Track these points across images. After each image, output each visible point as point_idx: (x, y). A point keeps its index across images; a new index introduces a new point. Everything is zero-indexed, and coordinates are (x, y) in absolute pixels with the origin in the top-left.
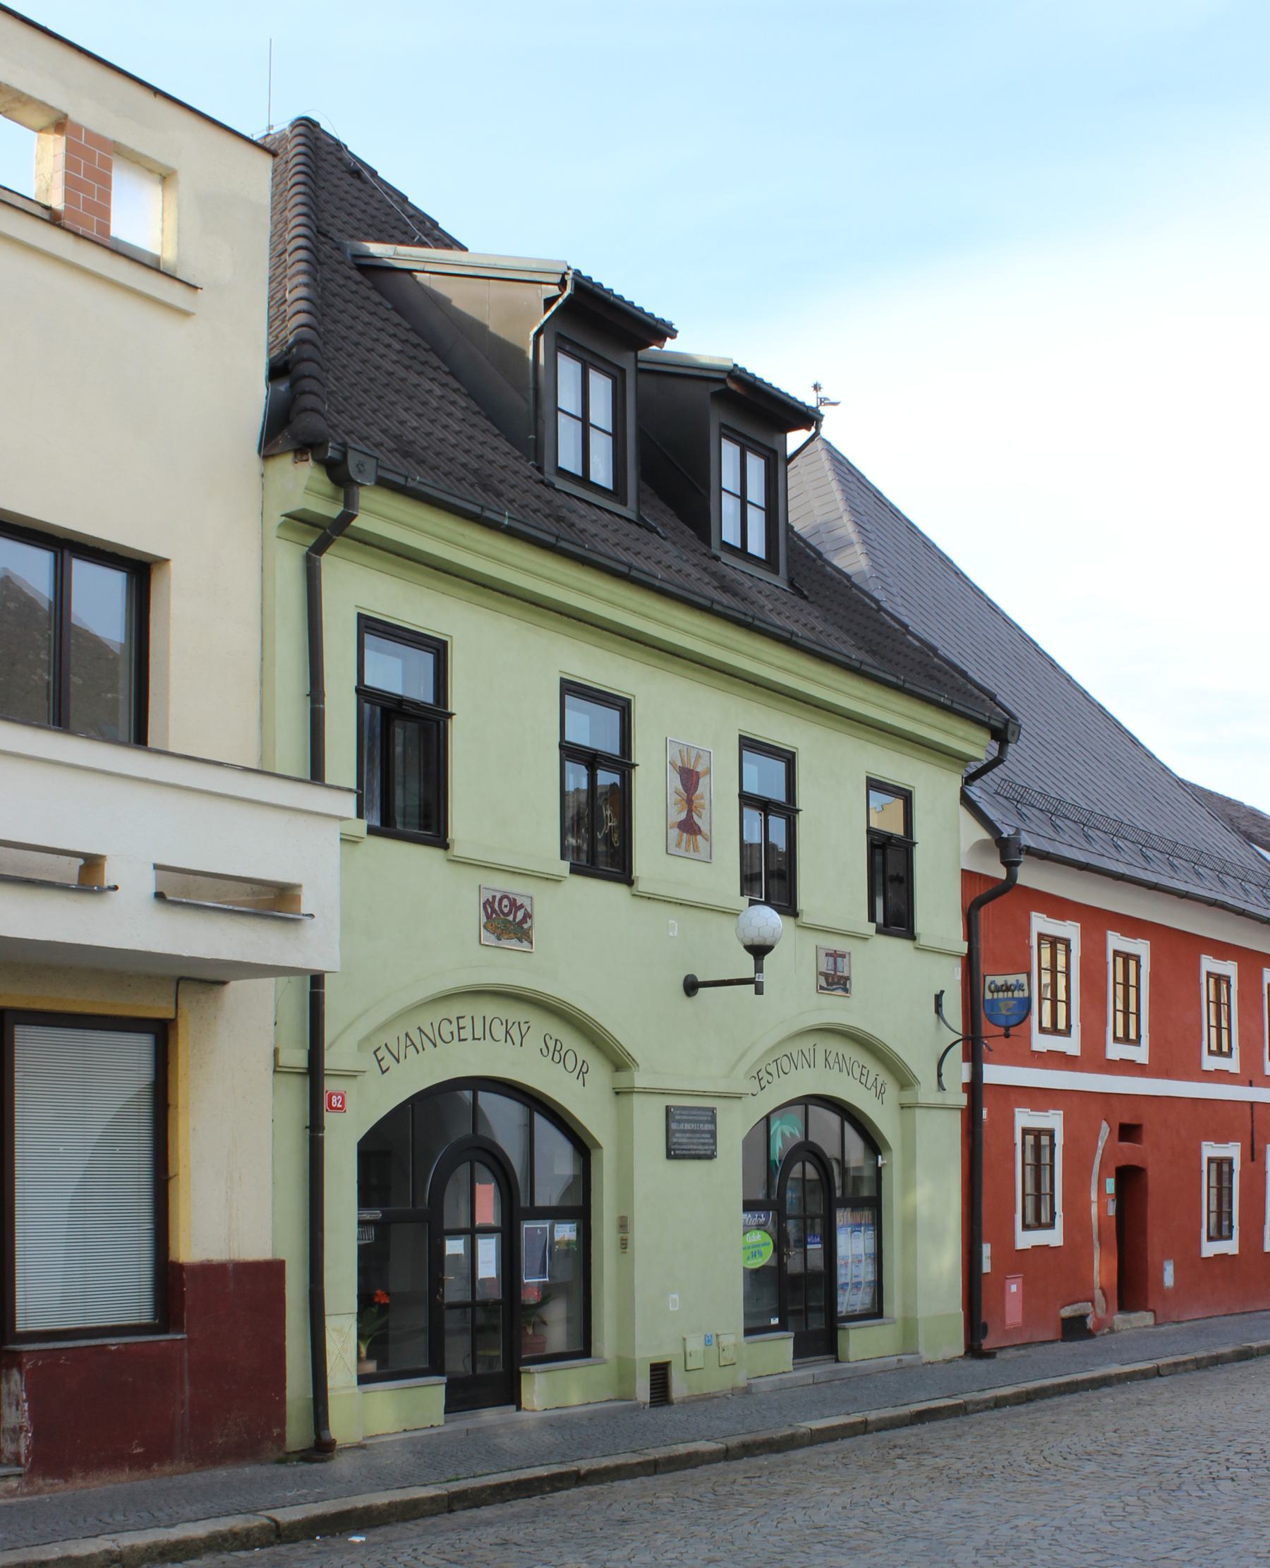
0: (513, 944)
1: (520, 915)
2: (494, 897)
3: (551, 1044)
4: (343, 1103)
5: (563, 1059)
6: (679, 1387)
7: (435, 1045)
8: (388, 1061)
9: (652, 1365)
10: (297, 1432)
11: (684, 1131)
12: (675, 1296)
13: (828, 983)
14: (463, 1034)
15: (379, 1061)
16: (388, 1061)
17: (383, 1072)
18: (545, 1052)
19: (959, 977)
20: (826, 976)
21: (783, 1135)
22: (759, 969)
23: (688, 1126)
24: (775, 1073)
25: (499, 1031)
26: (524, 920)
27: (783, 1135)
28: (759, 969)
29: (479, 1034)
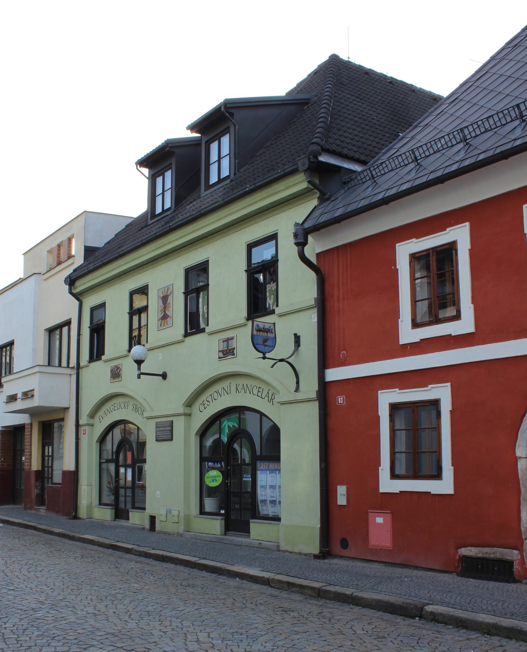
3: (135, 406)
5: (138, 411)
11: (160, 431)
12: (158, 492)
13: (224, 355)
19: (316, 320)
20: (223, 351)
21: (229, 427)
22: (139, 369)
23: (161, 429)
24: (211, 401)
27: (229, 427)
28: (139, 369)
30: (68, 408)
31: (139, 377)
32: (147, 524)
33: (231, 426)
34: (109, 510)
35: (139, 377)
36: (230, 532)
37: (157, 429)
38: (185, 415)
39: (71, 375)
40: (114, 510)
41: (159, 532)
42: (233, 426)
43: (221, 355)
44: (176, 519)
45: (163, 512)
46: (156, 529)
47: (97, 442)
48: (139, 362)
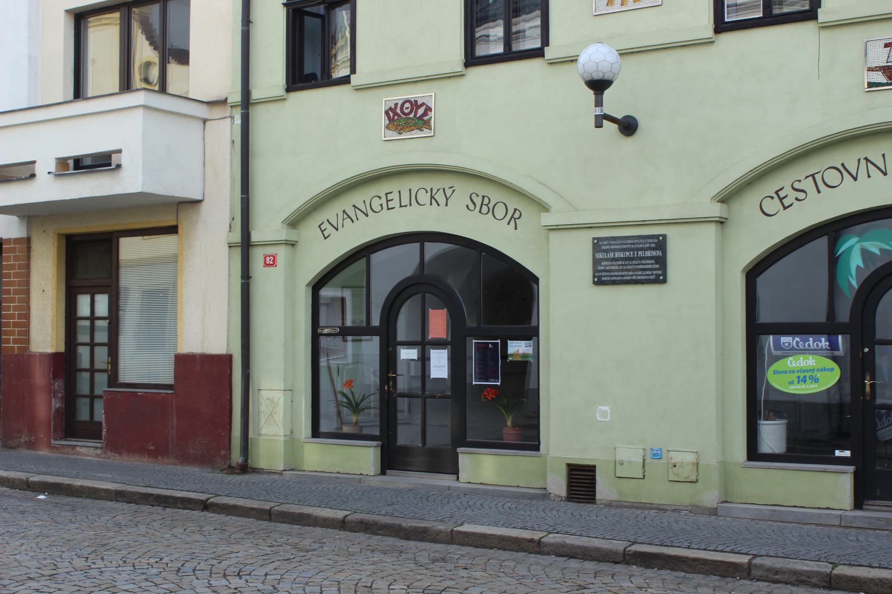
0: (416, 134)
1: (421, 111)
2: (396, 105)
3: (478, 201)
4: (274, 261)
6: (604, 489)
7: (367, 215)
8: (330, 230)
9: (569, 465)
10: (236, 457)
14: (391, 205)
15: (322, 231)
16: (330, 230)
17: (325, 238)
18: (471, 206)
22: (599, 103)
25: (424, 198)
26: (425, 114)
27: (865, 253)
28: (599, 103)
29: (405, 201)
30: (200, 201)
31: (599, 125)
32: (558, 485)
33: (877, 252)
34: (372, 449)
35: (599, 125)
36: (871, 502)
37: (599, 256)
38: (721, 222)
39: (205, 121)
40: (379, 449)
41: (609, 505)
42: (881, 250)
43: (880, 77)
44: (687, 472)
45: (630, 455)
46: (598, 497)
47: (307, 285)
48: (599, 86)
